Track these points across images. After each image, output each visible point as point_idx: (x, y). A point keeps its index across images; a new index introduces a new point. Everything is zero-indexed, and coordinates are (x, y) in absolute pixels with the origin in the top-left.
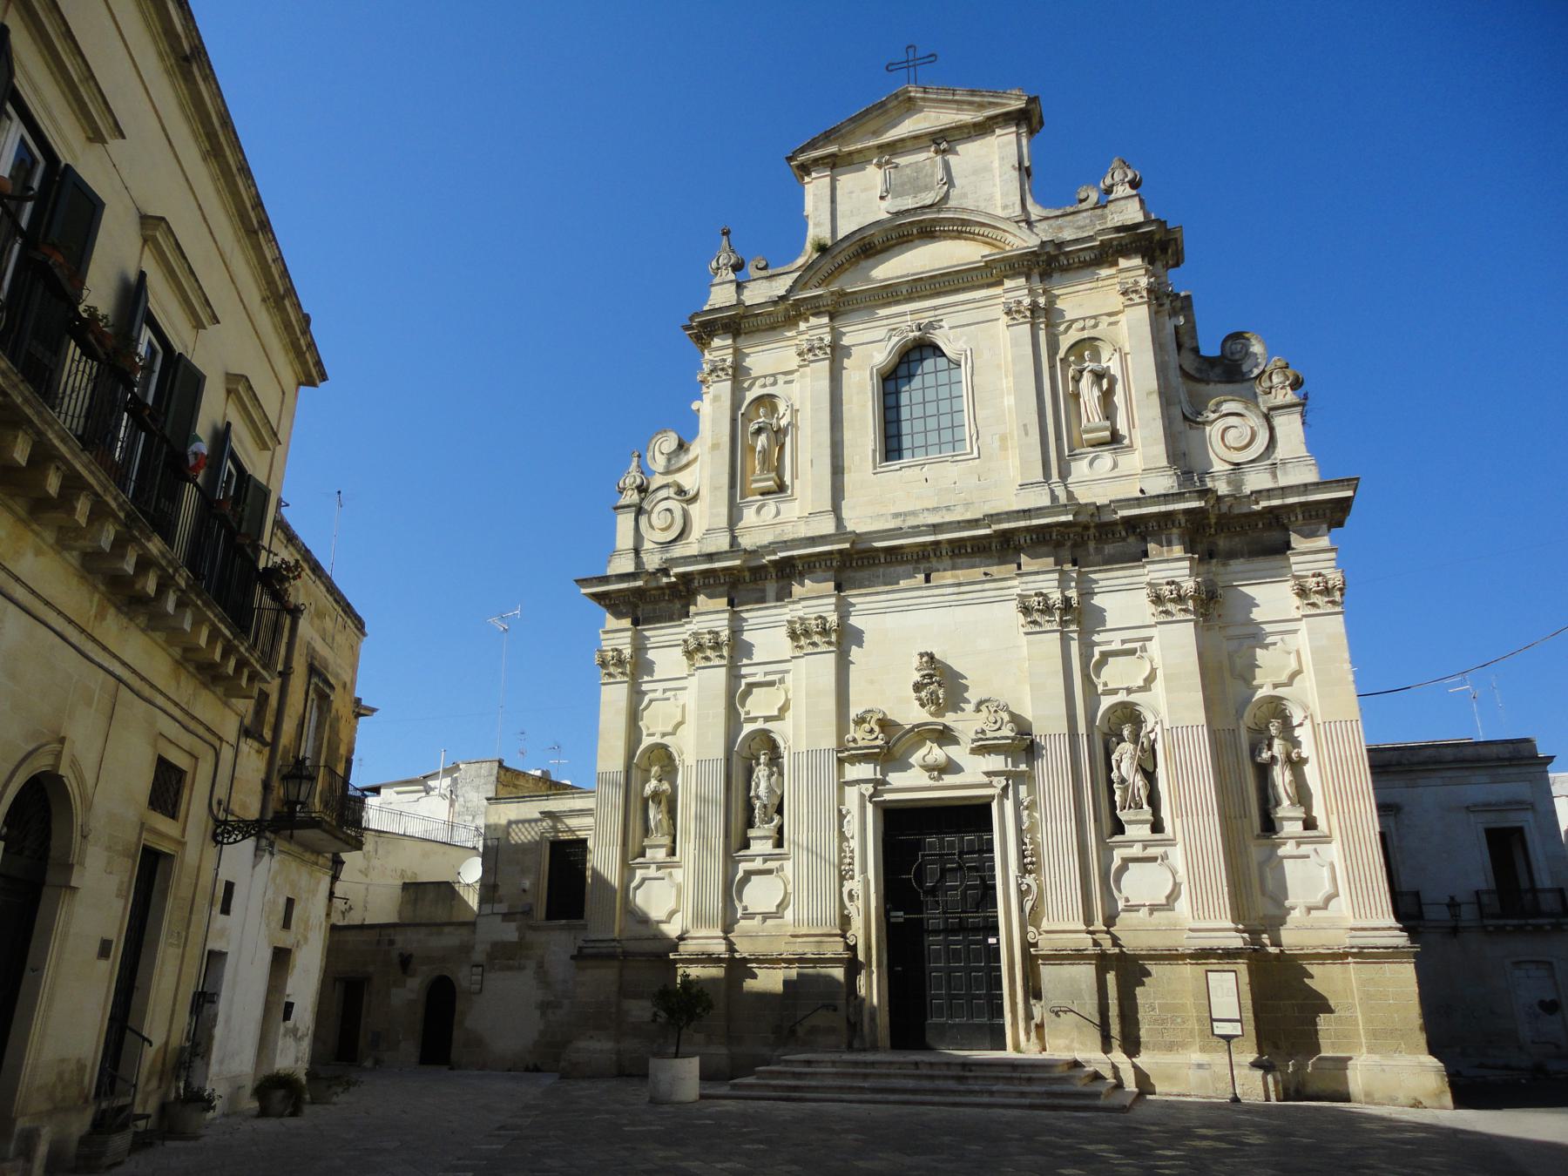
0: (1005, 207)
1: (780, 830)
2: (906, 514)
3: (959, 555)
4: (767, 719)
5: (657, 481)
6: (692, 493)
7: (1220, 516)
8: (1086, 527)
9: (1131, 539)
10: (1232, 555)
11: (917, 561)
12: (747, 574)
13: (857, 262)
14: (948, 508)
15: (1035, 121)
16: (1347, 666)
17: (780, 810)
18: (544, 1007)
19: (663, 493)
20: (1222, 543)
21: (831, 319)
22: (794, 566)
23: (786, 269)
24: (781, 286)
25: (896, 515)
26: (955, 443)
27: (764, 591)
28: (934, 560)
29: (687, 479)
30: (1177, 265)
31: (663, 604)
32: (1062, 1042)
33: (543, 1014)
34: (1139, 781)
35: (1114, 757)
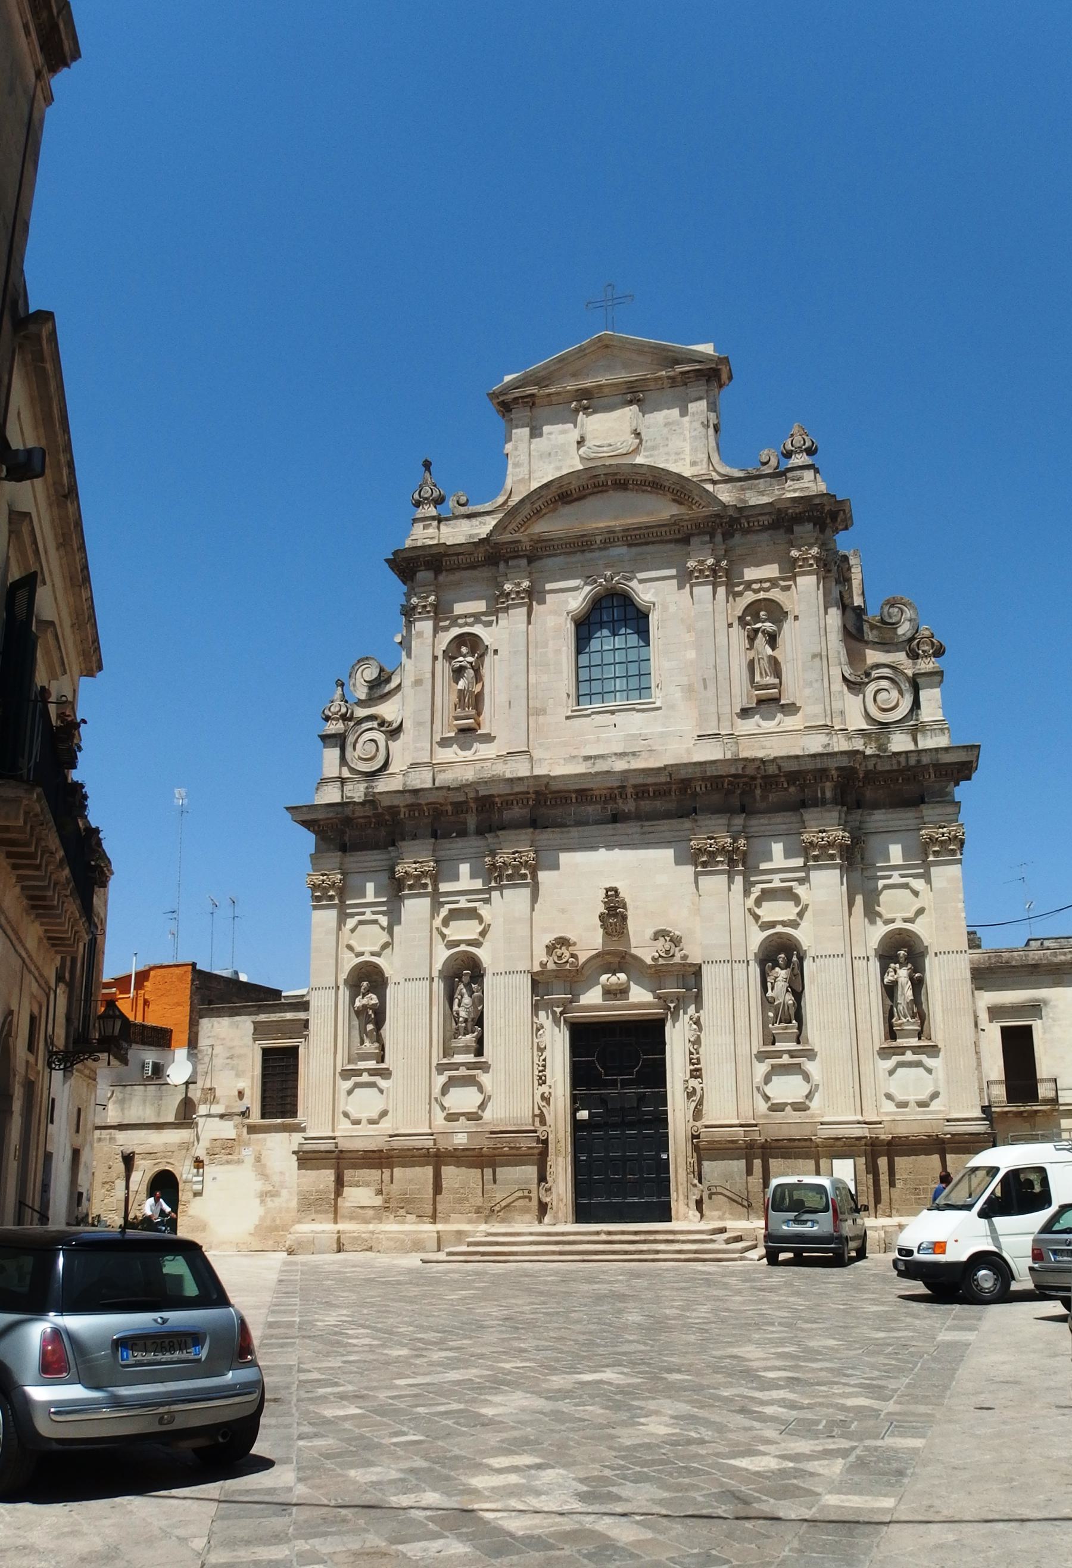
0: (693, 464)
1: (480, 1041)
2: (596, 757)
3: (643, 798)
4: (469, 943)
5: (361, 712)
6: (395, 725)
7: (867, 773)
8: (753, 778)
9: (792, 789)
10: (876, 806)
11: (605, 802)
12: (449, 808)
13: (554, 510)
14: (634, 754)
15: (724, 376)
16: (961, 905)
17: (479, 1021)
18: (264, 1196)
19: (366, 725)
20: (869, 794)
21: (530, 562)
22: (494, 803)
23: (487, 507)
24: (483, 528)
25: (587, 758)
26: (643, 690)
27: (465, 823)
28: (620, 801)
29: (388, 710)
30: (846, 528)
31: (369, 831)
32: (716, 1213)
33: (262, 1202)
34: (790, 999)
35: (770, 979)
